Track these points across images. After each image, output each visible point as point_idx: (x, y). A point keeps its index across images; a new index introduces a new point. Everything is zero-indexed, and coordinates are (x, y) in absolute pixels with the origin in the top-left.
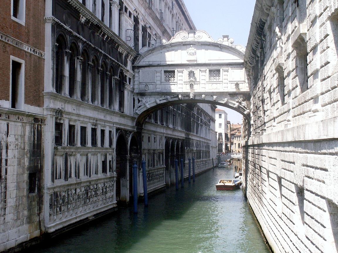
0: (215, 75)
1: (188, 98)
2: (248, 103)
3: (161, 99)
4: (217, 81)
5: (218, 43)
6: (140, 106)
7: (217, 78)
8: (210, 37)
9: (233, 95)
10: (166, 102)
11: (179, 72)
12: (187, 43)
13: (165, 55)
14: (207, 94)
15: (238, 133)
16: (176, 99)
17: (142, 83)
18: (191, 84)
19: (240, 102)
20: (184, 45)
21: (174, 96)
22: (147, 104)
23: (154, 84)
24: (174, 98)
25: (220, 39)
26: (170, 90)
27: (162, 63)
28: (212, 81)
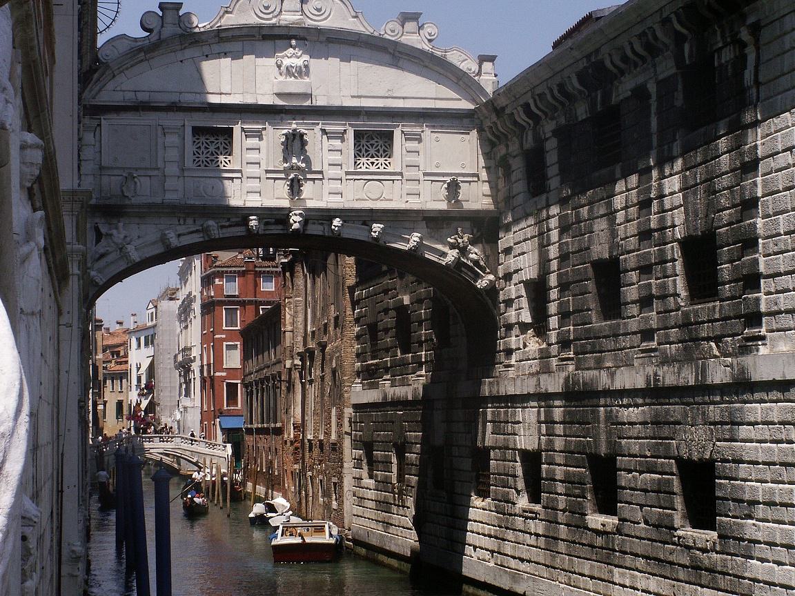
0: (372, 151)
1: (280, 227)
2: (489, 252)
3: (181, 229)
4: (381, 170)
5: (386, 36)
6: (102, 256)
7: (382, 160)
8: (356, 17)
9: (435, 222)
10: (201, 240)
11: (248, 134)
12: (276, 32)
13: (199, 71)
14: (349, 215)
15: (113, 365)
16: (239, 231)
17: (108, 168)
18: (292, 180)
19: (461, 245)
20: (265, 38)
21: (229, 220)
22: (130, 248)
23: (156, 173)
24: (230, 226)
25: (390, 26)
26: (224, 196)
27: (188, 99)
28: (364, 169)
